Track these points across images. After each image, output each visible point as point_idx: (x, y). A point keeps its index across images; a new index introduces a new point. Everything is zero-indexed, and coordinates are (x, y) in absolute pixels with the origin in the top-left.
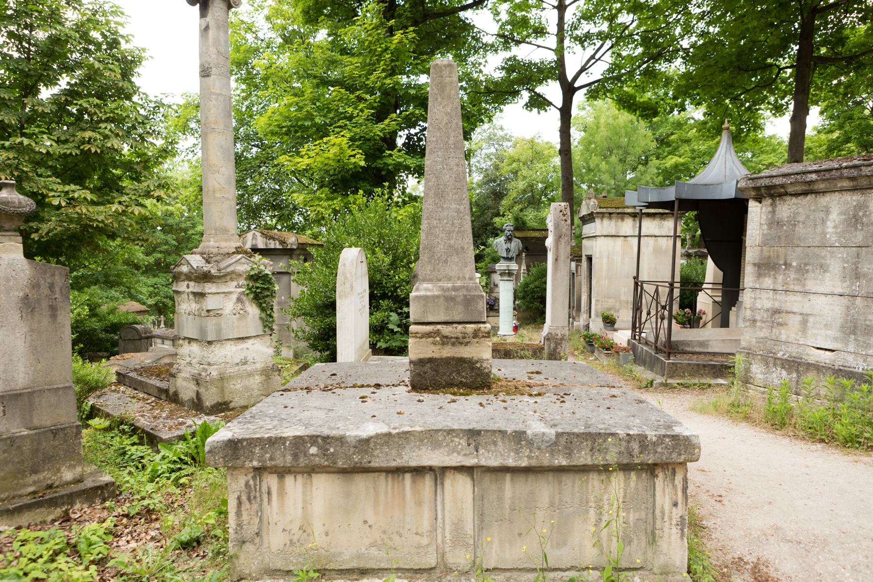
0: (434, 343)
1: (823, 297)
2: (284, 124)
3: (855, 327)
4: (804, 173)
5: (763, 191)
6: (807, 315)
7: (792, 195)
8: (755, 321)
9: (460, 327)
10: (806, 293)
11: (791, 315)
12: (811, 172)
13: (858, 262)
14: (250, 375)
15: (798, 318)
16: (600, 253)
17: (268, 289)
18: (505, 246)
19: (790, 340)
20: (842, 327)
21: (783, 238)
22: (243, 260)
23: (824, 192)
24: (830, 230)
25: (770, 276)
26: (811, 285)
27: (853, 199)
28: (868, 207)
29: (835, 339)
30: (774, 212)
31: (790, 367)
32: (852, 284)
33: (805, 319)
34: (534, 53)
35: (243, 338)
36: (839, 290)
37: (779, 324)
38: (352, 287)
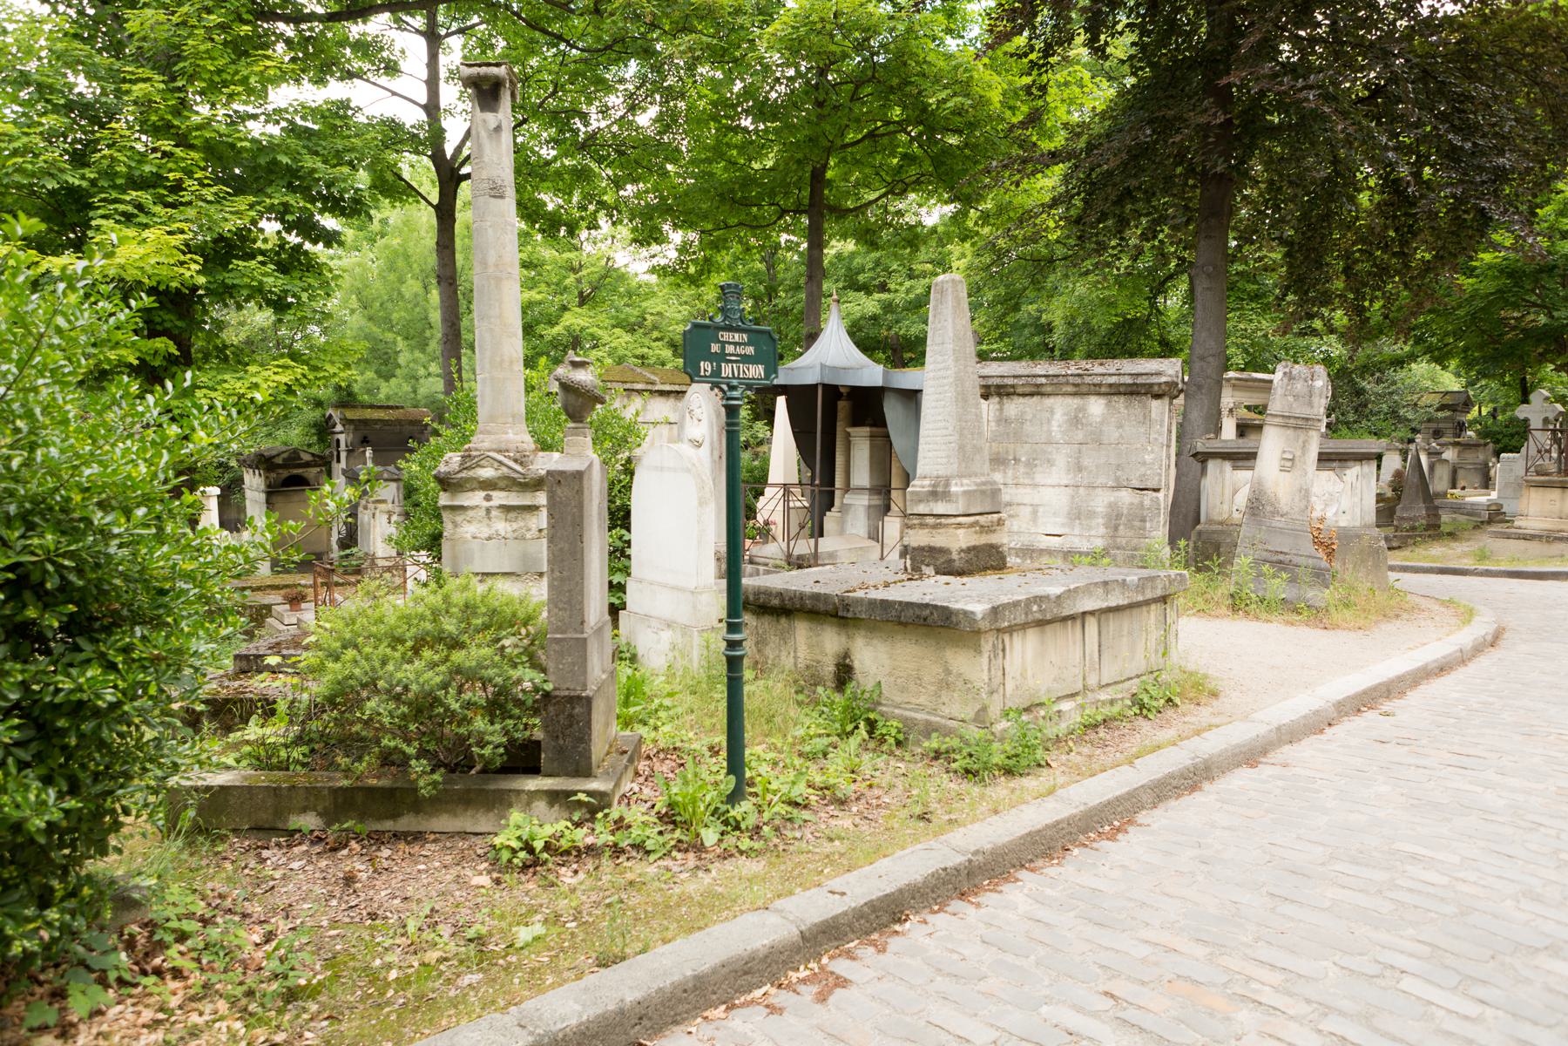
15: (1029, 509)
26: (1039, 478)
27: (1075, 402)
29: (1063, 525)
30: (1001, 410)
33: (1035, 509)
36: (1065, 482)
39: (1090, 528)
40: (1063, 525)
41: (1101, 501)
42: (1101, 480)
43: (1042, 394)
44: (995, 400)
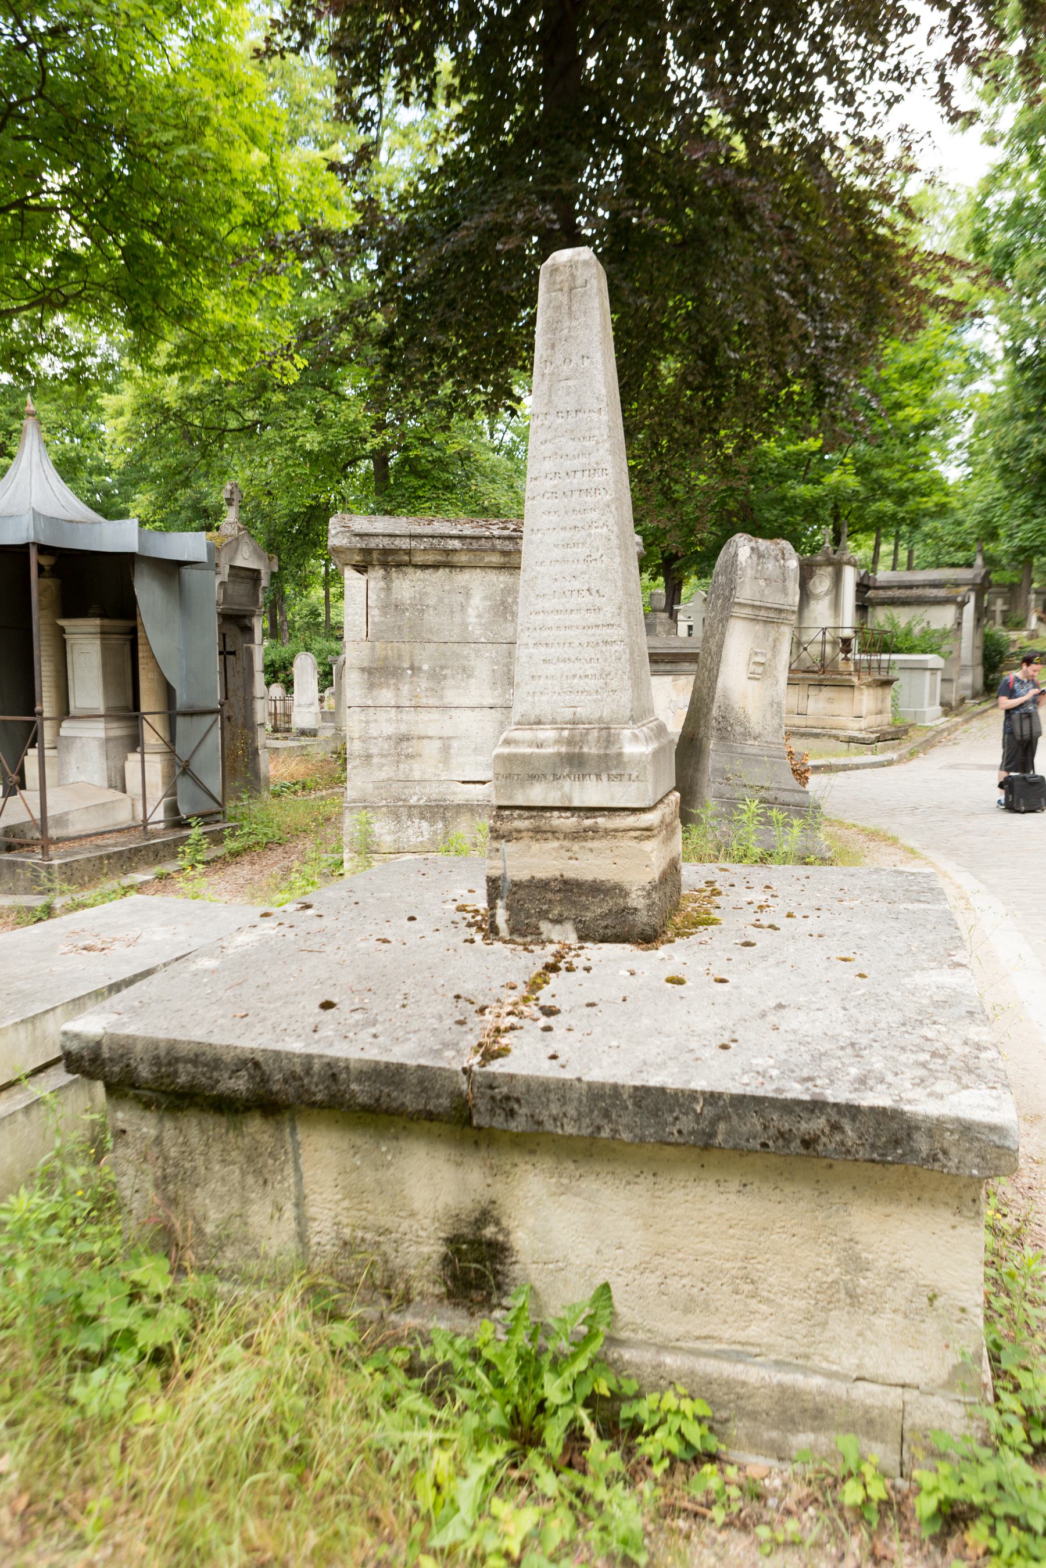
1: (469, 712)
4: (442, 537)
5: (375, 555)
7: (416, 566)
8: (369, 757)
12: (451, 537)
15: (438, 744)
21: (406, 630)
24: (472, 620)
25: (388, 686)
26: (451, 697)
30: (388, 589)
31: (433, 815)
33: (446, 744)
36: (490, 701)
37: (409, 756)
43: (451, 566)
44: (377, 574)
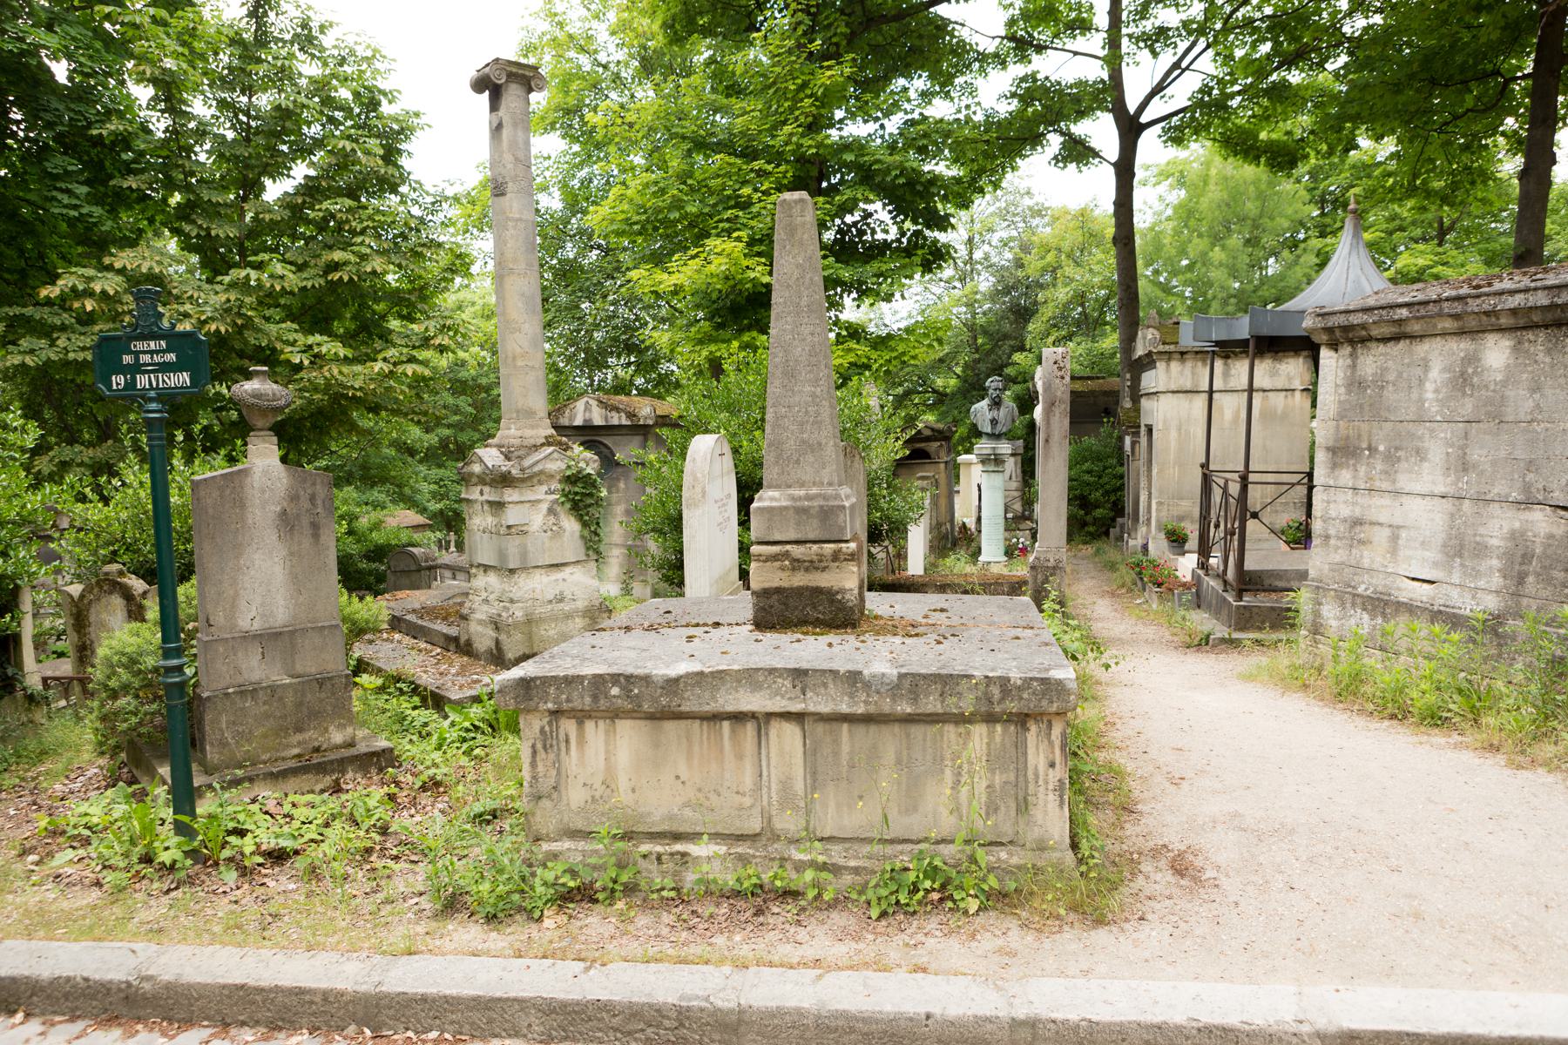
0: (782, 569)
1: (1419, 499)
2: (636, 218)
3: (1462, 546)
5: (1338, 333)
6: (1398, 527)
7: (1378, 340)
8: (1327, 537)
9: (815, 547)
10: (1397, 493)
11: (1376, 528)
12: (1400, 306)
13: (1466, 446)
14: (568, 616)
15: (1386, 532)
16: (1165, 421)
17: (591, 495)
18: (989, 416)
19: (1375, 566)
20: (1444, 546)
21: (1367, 408)
22: (556, 455)
23: (1422, 337)
24: (1430, 395)
28: (1479, 360)
29: (1436, 564)
30: (1354, 366)
32: (1458, 480)
34: (1069, 64)
35: (557, 565)
37: (1359, 541)
38: (704, 493)
39: (1477, 574)
40: (1436, 564)
41: (1498, 526)
42: (1498, 489)
43: (1411, 337)
44: (1346, 350)
